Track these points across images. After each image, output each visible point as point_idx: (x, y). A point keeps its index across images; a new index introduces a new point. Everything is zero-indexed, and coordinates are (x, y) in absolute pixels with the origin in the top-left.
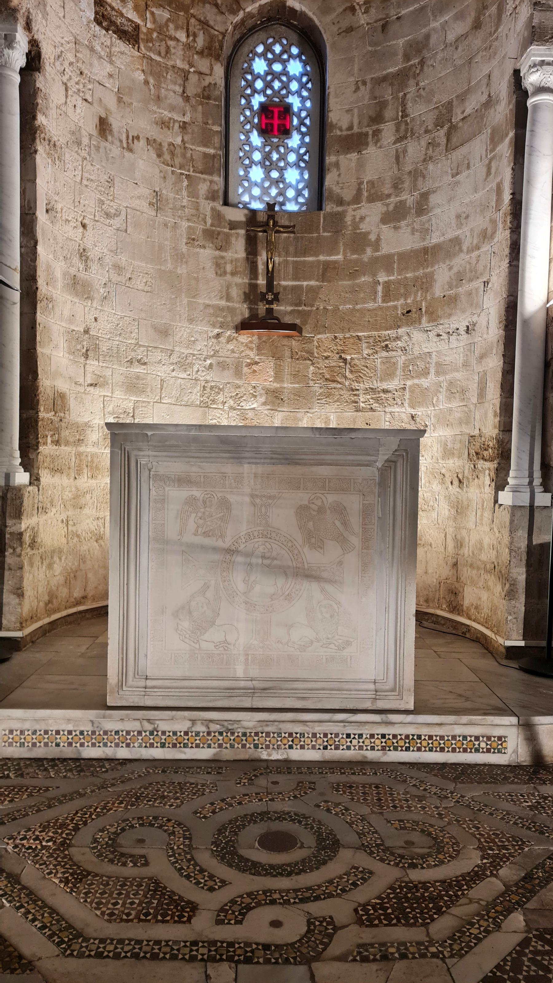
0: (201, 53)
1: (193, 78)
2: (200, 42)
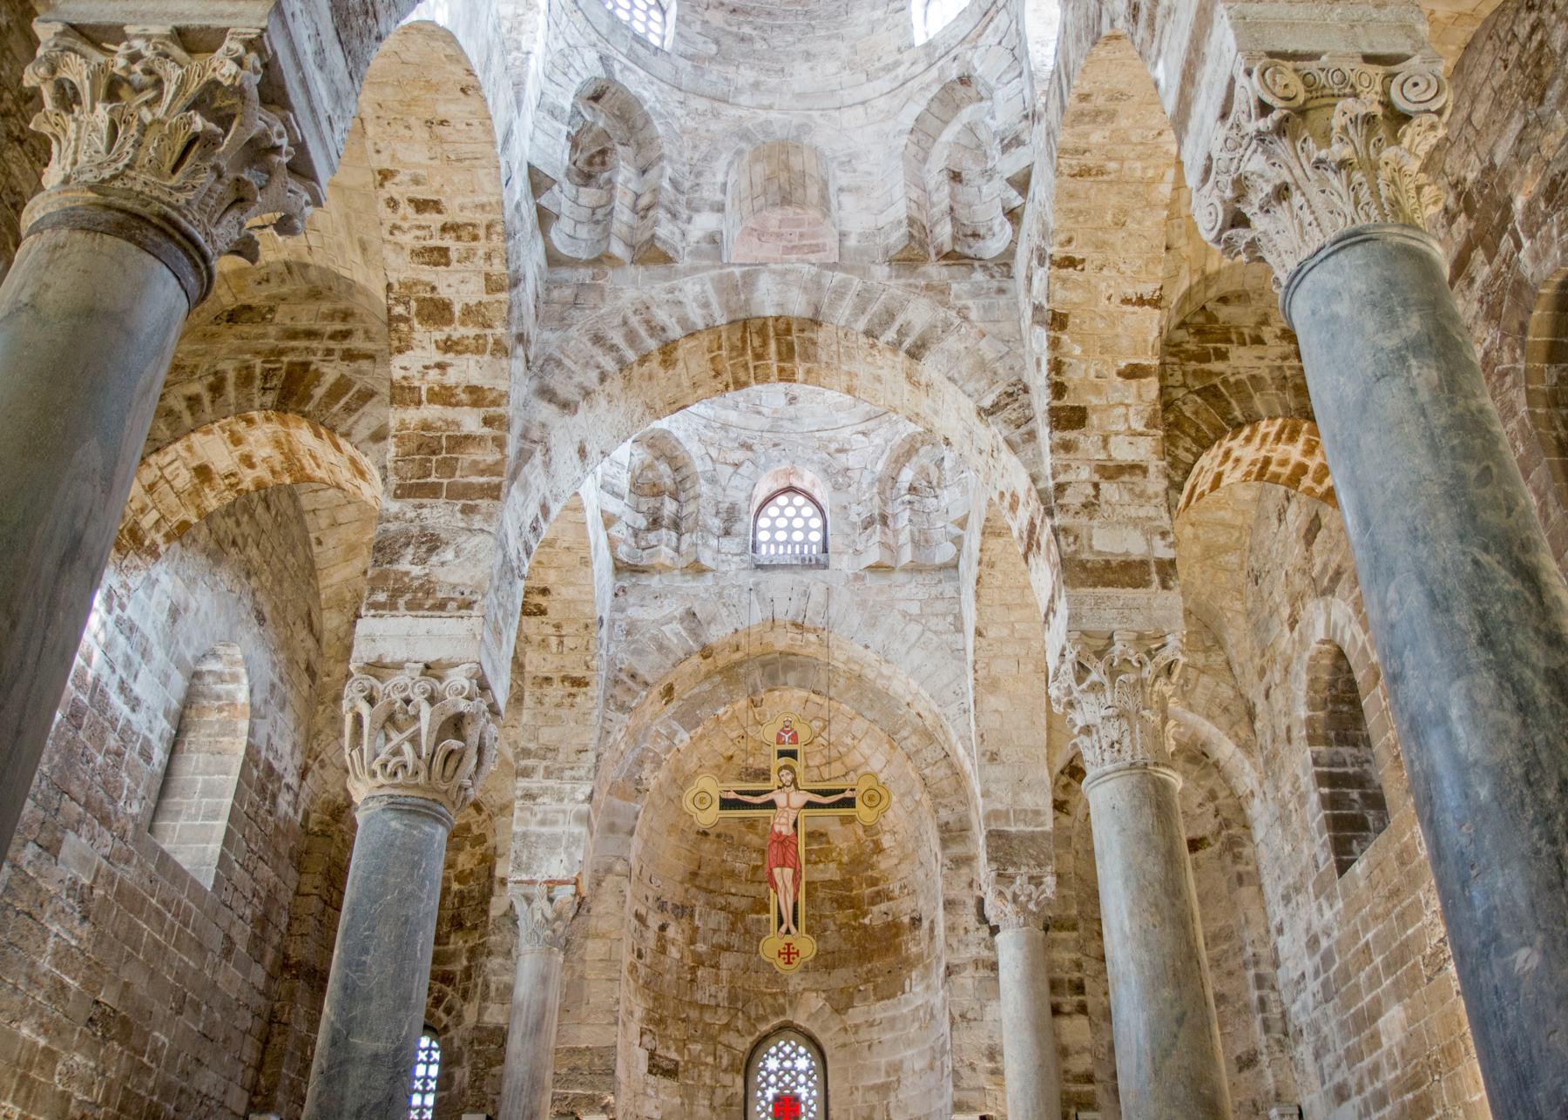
0: (725, 1071)
1: (719, 1091)
2: (725, 1062)
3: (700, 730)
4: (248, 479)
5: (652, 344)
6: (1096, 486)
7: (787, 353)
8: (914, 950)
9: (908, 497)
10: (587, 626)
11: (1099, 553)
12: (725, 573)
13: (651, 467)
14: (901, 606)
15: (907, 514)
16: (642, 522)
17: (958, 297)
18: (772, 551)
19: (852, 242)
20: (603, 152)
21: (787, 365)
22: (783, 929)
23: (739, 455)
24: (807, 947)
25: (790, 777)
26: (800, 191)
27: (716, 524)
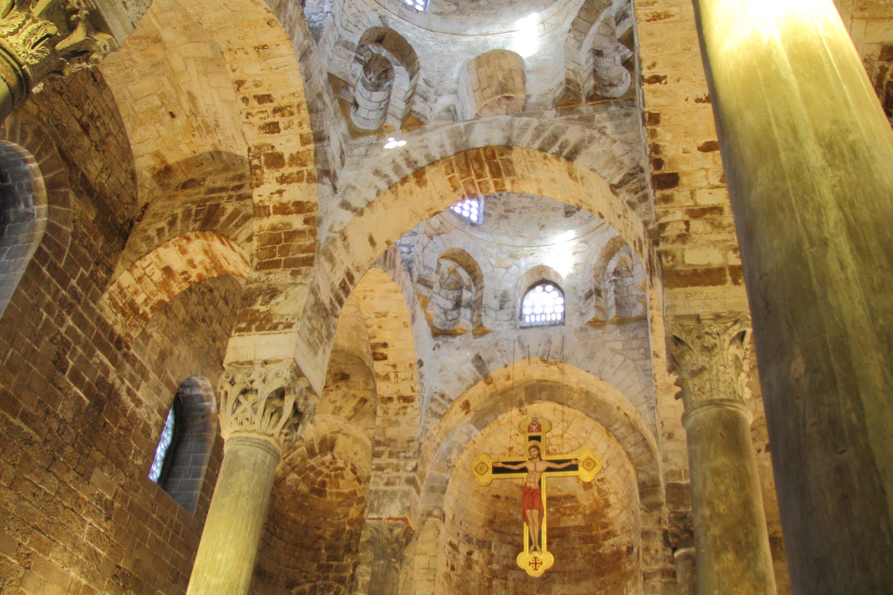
3: (487, 429)
4: (194, 274)
5: (409, 171)
6: (687, 223)
7: (496, 173)
8: (629, 568)
9: (613, 278)
10: (411, 365)
11: (690, 265)
12: (500, 332)
13: (454, 271)
14: (610, 345)
15: (613, 287)
16: (449, 305)
17: (599, 122)
19: (533, 100)
20: (386, 72)
22: (532, 548)
23: (509, 262)
24: (547, 559)
25: (536, 453)
26: (511, 82)
27: (495, 303)
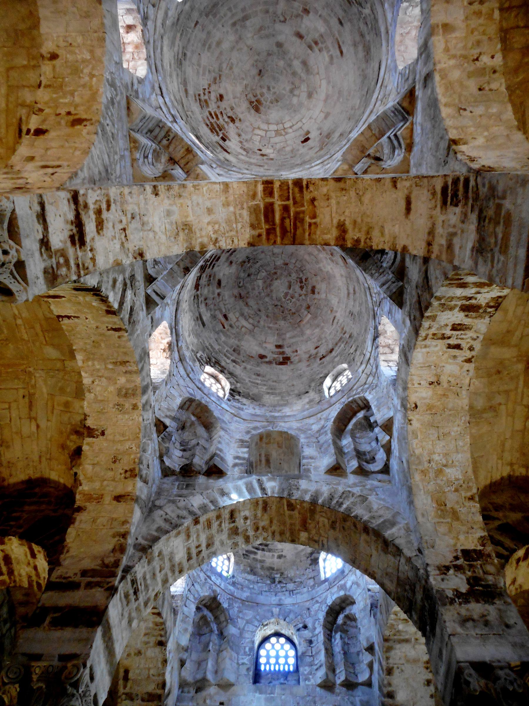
7: (269, 209)
18: (268, 669)
21: (269, 200)
